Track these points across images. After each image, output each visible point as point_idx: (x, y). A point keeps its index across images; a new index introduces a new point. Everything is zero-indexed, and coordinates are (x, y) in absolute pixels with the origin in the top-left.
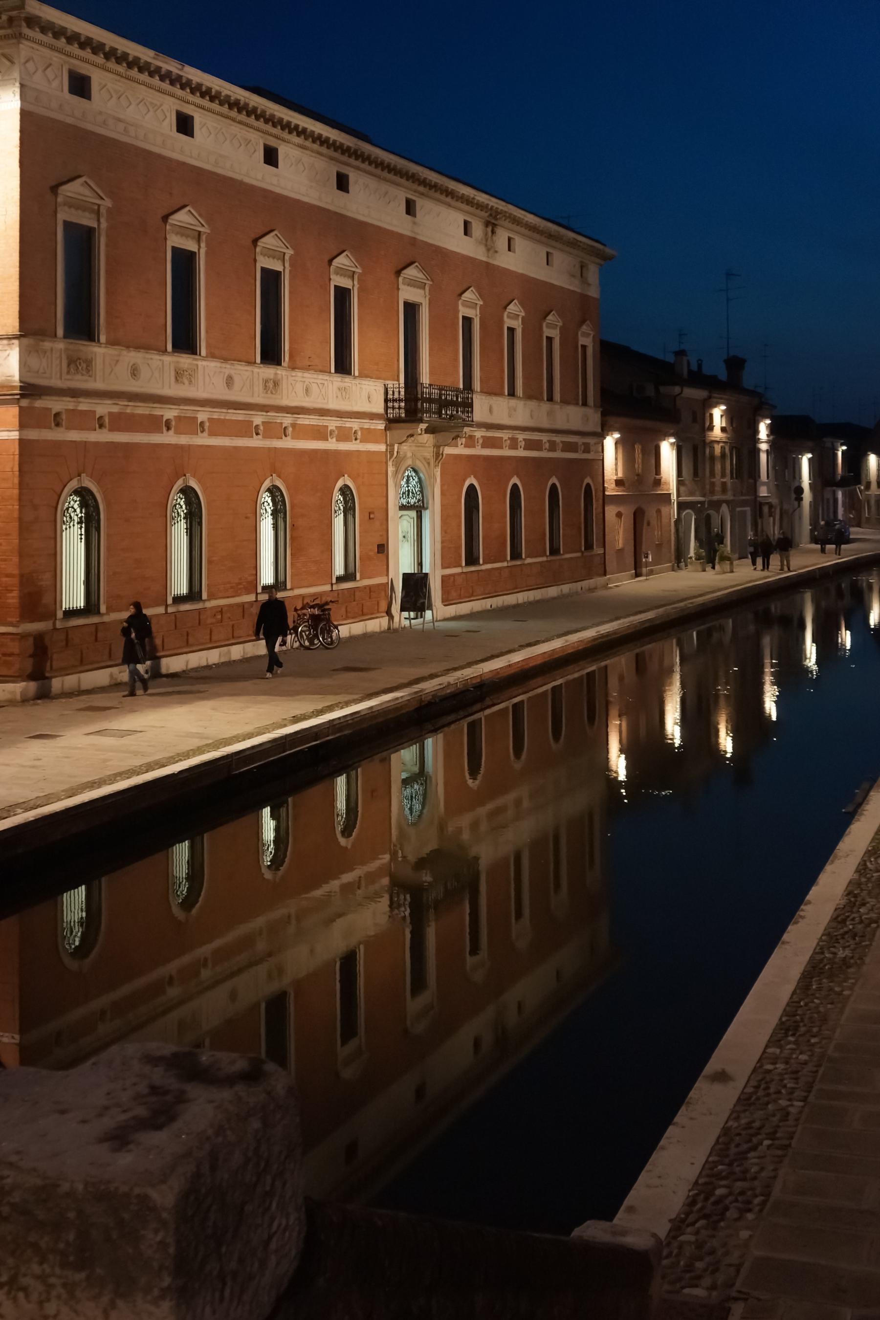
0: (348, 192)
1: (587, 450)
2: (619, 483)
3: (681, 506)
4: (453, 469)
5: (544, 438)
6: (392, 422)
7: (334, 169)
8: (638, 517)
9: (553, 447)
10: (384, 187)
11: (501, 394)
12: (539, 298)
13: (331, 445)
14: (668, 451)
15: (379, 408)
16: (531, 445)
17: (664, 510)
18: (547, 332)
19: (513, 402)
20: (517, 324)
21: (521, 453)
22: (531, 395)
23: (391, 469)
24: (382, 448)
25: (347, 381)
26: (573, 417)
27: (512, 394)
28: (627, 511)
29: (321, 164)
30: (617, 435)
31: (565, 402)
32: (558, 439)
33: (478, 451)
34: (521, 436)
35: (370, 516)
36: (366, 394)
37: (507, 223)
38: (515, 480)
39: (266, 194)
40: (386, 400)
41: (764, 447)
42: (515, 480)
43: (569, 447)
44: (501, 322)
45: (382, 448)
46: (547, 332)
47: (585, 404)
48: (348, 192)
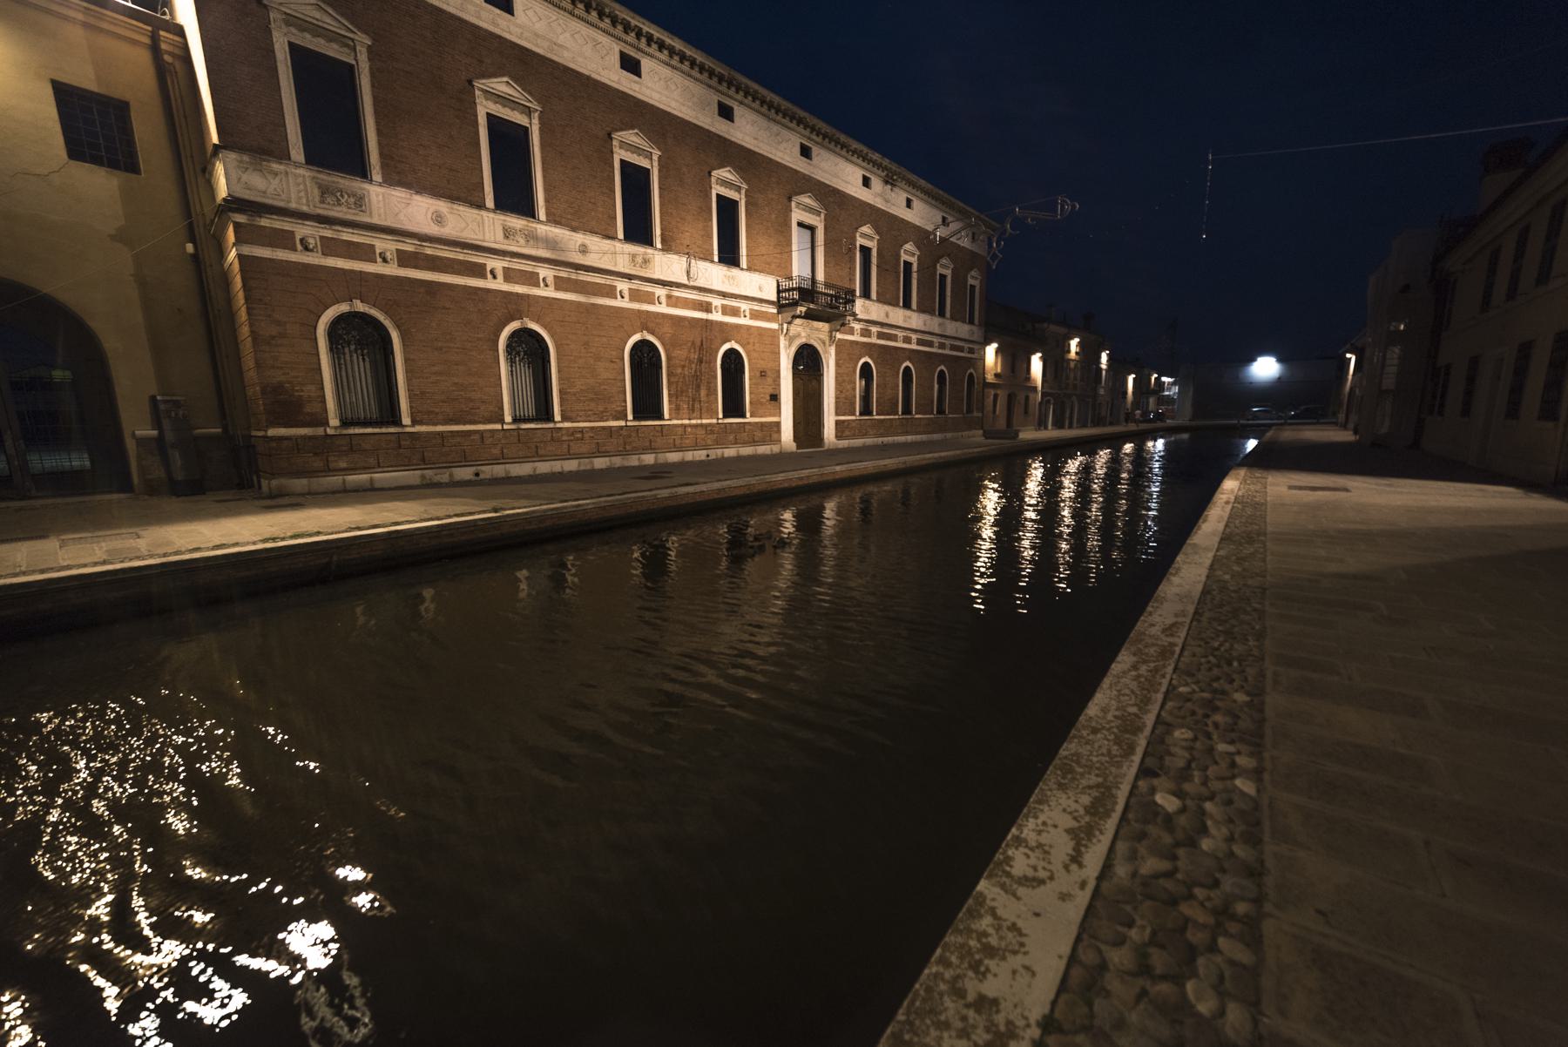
0: (732, 121)
1: (971, 351)
2: (996, 375)
3: (1043, 394)
4: (841, 346)
5: (936, 340)
6: (781, 306)
7: (715, 98)
8: (1011, 398)
9: (942, 346)
10: (776, 128)
11: (897, 305)
12: (932, 248)
13: (716, 316)
14: (1036, 365)
15: (774, 298)
16: (920, 342)
17: (1032, 396)
18: (940, 270)
19: (908, 313)
20: (914, 260)
21: (914, 347)
22: (922, 309)
23: (783, 342)
24: (775, 326)
25: (735, 271)
26: (962, 329)
27: (907, 305)
28: (1002, 395)
29: (697, 89)
30: (995, 345)
31: (953, 318)
32: (948, 342)
33: (874, 340)
34: (914, 337)
35: (763, 374)
36: (763, 286)
37: (903, 184)
38: (908, 363)
39: (625, 96)
40: (779, 292)
41: (1104, 367)
42: (908, 363)
43: (953, 348)
44: (898, 256)
45: (775, 326)
46: (940, 270)
47: (971, 322)
48: (732, 121)
